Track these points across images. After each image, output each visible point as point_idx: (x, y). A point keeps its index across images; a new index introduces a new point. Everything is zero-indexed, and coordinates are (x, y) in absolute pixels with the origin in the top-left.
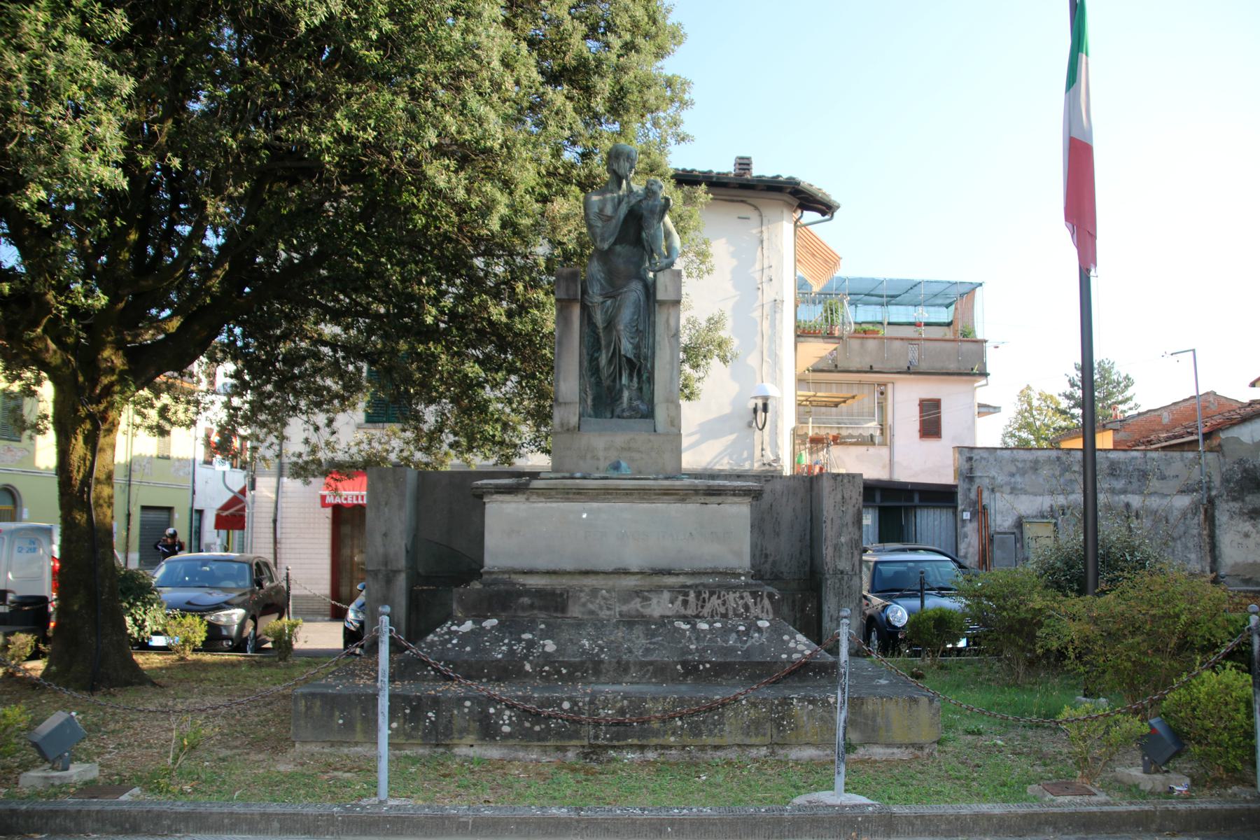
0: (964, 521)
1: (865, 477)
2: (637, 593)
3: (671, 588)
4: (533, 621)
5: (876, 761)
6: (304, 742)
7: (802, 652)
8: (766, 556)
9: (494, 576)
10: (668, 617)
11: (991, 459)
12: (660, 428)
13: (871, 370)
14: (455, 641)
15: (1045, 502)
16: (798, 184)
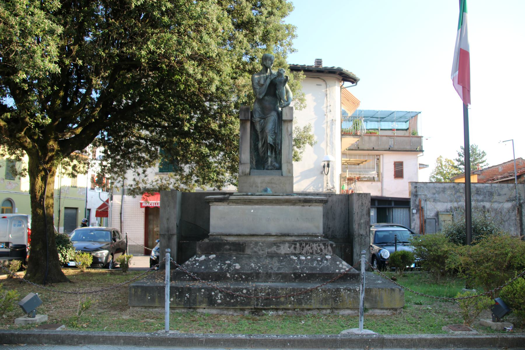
0: (413, 214)
1: (371, 195)
2: (275, 244)
3: (289, 242)
4: (231, 256)
5: (376, 316)
6: (134, 306)
7: (345, 269)
8: (329, 228)
9: (214, 237)
10: (288, 254)
11: (425, 187)
12: (284, 174)
13: (373, 149)
14: (197, 264)
15: (448, 205)
16: (342, 70)
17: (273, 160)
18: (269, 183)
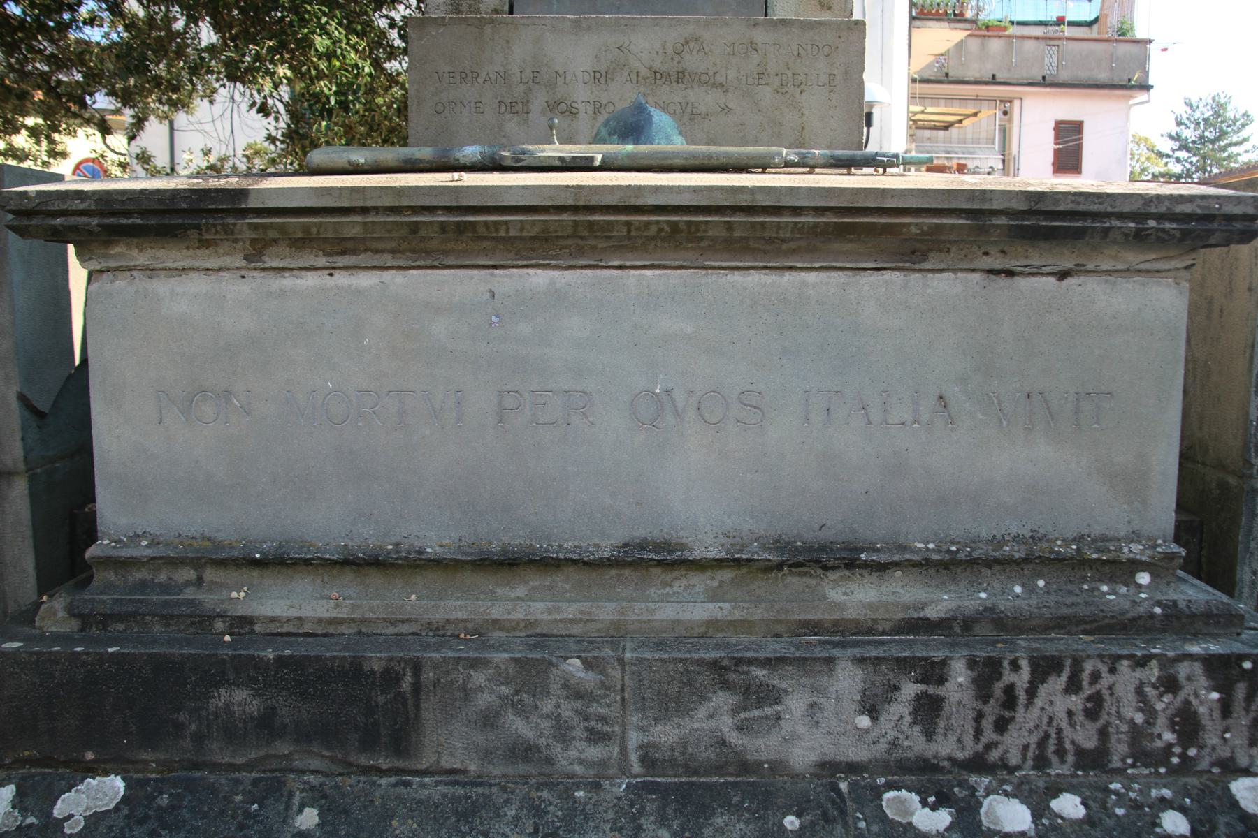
9: (137, 576)
10: (852, 768)
13: (993, 81)
18: (658, 75)
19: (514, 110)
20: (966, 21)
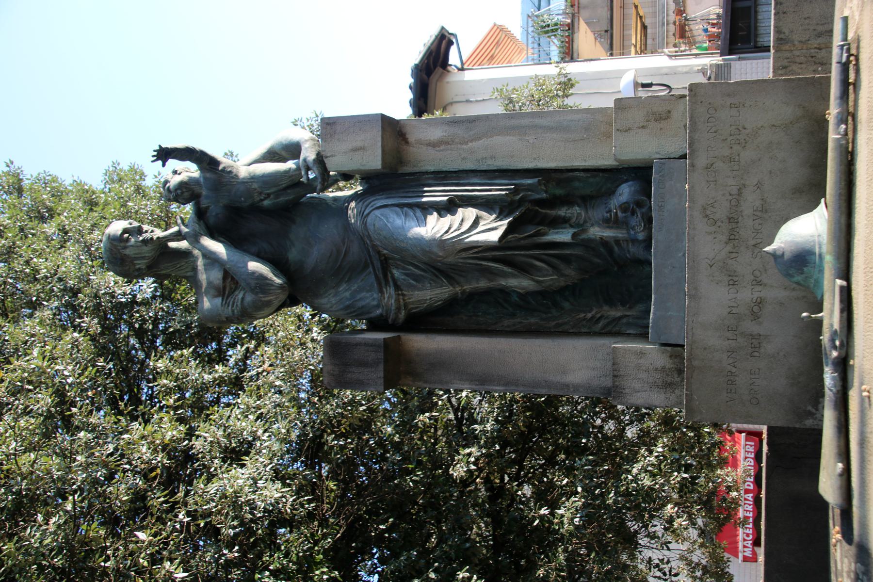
12: (676, 145)
16: (417, 66)
17: (598, 213)
19: (758, 346)
20: (573, 21)
